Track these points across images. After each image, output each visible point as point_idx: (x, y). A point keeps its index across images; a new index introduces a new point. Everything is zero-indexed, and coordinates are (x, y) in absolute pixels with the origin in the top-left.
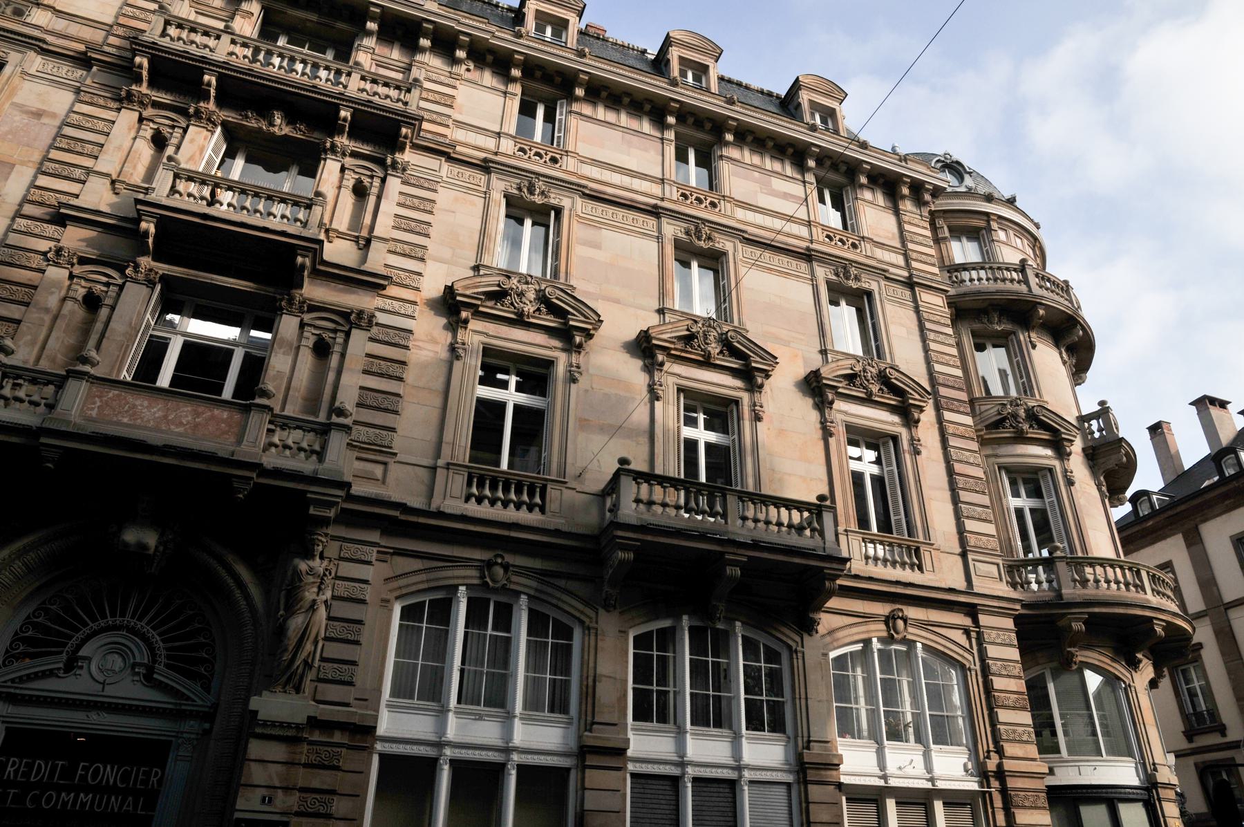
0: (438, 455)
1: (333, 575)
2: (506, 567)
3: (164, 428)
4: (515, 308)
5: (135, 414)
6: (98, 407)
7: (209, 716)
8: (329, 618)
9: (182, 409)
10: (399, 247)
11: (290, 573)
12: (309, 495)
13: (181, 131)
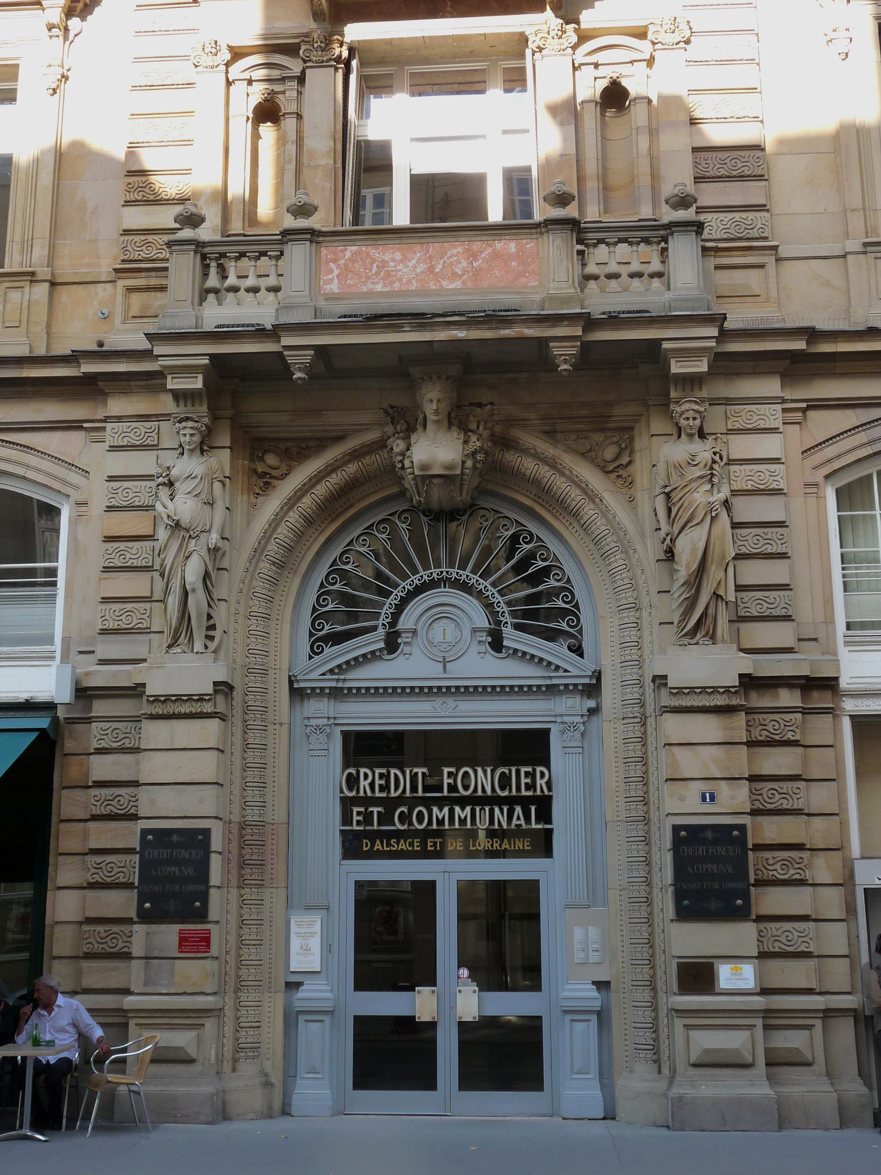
1: (725, 460)
3: (433, 287)
5: (388, 274)
6: (337, 276)
7: (593, 689)
8: (735, 526)
9: (449, 254)
11: (661, 467)
12: (666, 345)
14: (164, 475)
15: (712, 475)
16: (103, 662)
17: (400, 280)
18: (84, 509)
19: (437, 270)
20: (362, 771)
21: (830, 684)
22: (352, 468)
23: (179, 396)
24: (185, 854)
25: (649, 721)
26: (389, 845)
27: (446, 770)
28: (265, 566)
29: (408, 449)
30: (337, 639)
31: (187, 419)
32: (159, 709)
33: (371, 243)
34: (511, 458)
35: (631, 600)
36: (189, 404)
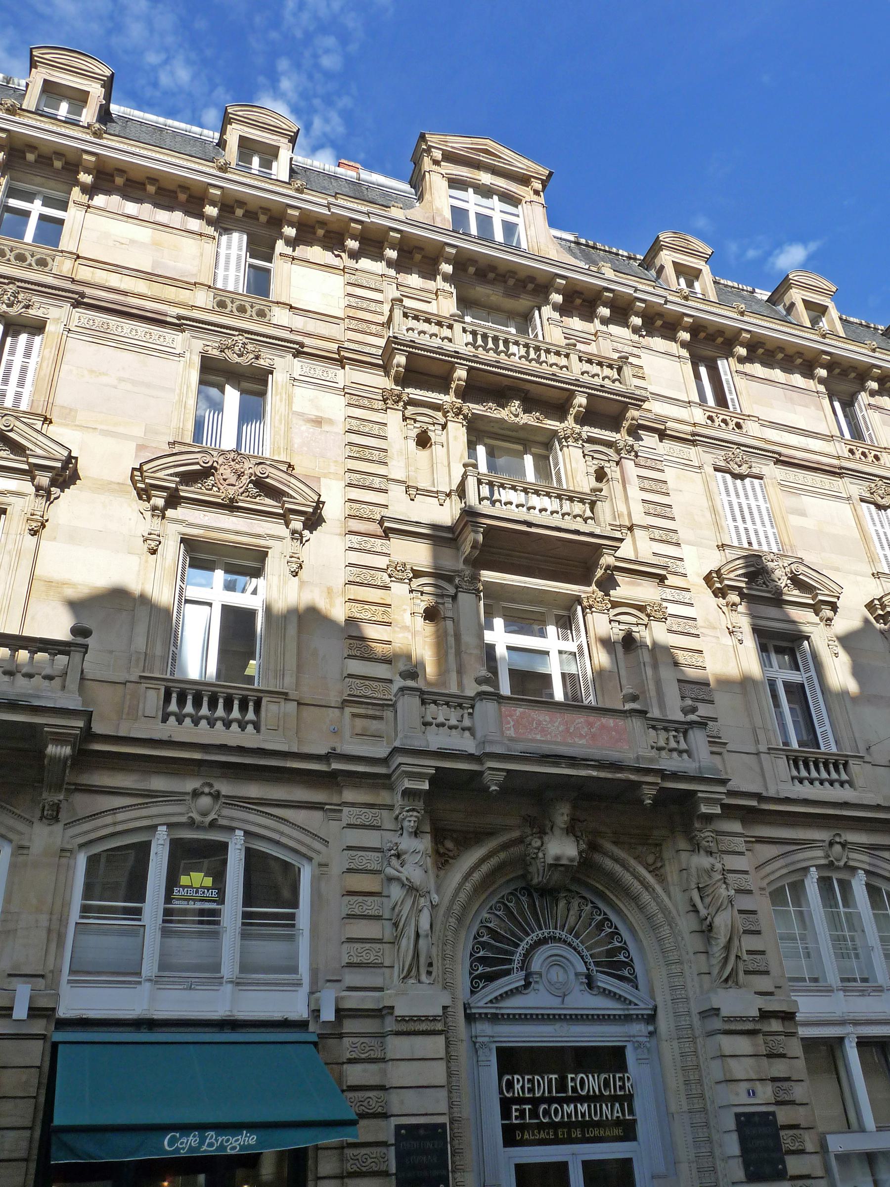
0: (757, 742)
2: (844, 845)
3: (570, 741)
4: (767, 586)
5: (543, 730)
7: (651, 1018)
10: (657, 534)
12: (700, 795)
13: (440, 427)
14: (395, 848)
15: (725, 878)
16: (350, 989)
17: (550, 734)
18: (325, 869)
19: (571, 731)
20: (516, 1077)
21: (788, 1017)
22: (502, 855)
23: (408, 793)
24: (429, 1145)
25: (698, 1040)
26: (533, 1135)
27: (570, 1076)
28: (453, 920)
29: (542, 845)
30: (490, 978)
31: (413, 810)
32: (404, 1027)
33: (531, 708)
34: (598, 858)
35: (676, 957)
36: (411, 800)
